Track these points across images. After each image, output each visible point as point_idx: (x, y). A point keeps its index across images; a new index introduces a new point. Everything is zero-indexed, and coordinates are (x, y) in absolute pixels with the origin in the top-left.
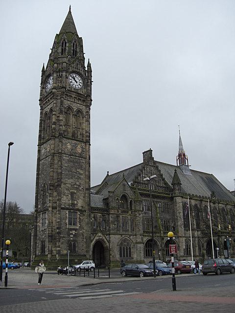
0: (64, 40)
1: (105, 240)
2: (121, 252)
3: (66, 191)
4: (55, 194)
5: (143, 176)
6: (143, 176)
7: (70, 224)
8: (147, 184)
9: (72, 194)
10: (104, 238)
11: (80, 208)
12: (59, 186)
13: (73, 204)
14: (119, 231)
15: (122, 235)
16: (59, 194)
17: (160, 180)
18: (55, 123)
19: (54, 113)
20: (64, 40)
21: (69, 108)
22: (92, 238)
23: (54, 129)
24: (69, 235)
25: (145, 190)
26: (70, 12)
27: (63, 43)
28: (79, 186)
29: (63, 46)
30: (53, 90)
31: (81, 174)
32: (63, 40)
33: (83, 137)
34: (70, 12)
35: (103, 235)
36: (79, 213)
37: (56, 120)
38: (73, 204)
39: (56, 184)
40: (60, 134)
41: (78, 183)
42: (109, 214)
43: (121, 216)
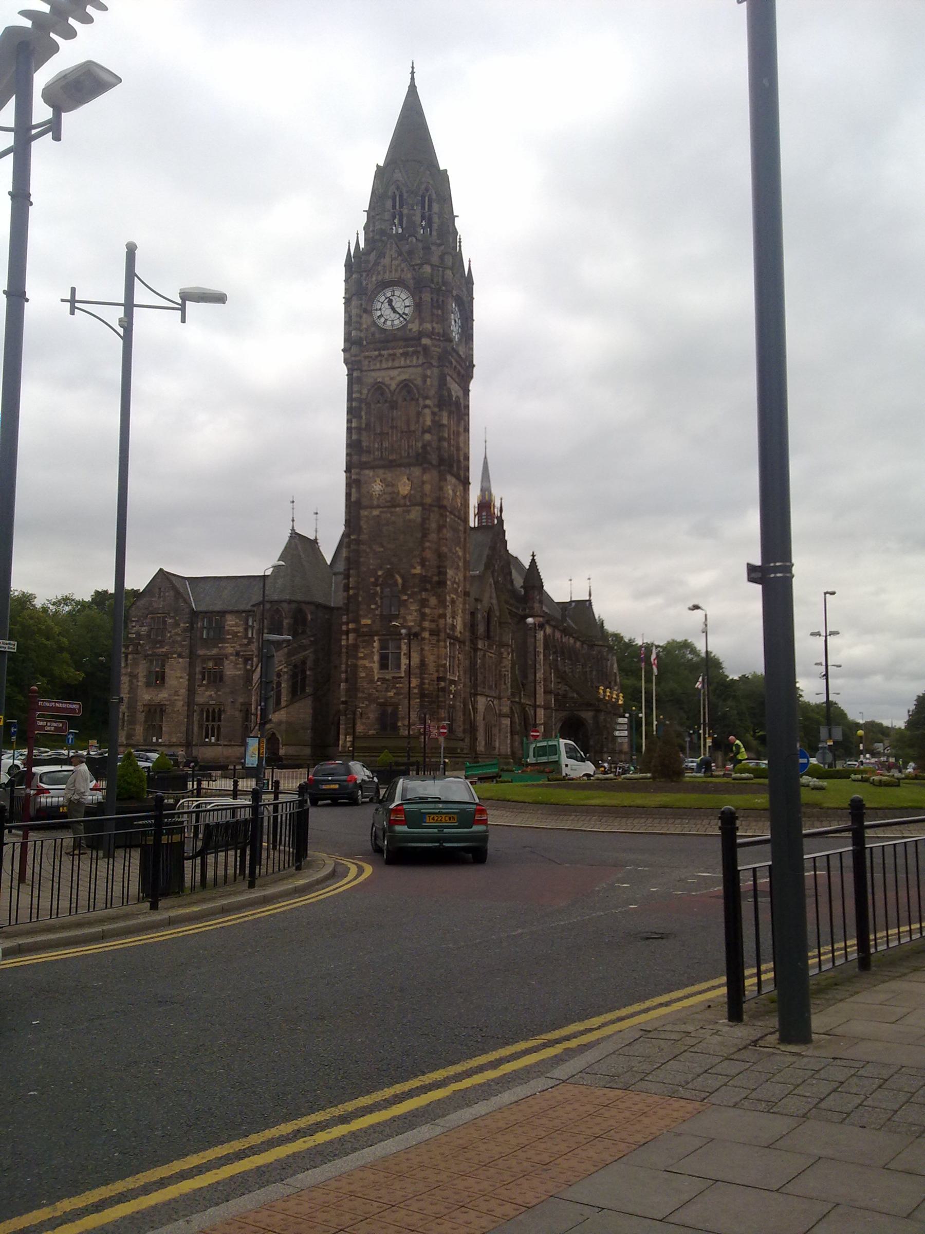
0: (427, 190)
4: (433, 601)
12: (442, 583)
16: (442, 603)
18: (428, 431)
19: (428, 402)
20: (427, 190)
23: (429, 443)
27: (423, 197)
29: (423, 207)
30: (425, 341)
32: (423, 187)
33: (459, 468)
37: (433, 421)
39: (436, 579)
40: (441, 461)
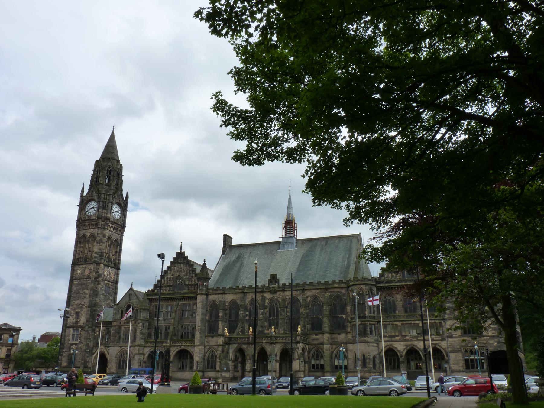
1: (106, 352)
2: (120, 364)
3: (72, 312)
5: (167, 278)
6: (167, 278)
7: (73, 339)
8: (171, 286)
9: (77, 314)
10: (105, 350)
11: (82, 325)
13: (77, 322)
14: (119, 342)
15: (121, 347)
17: (192, 277)
21: (84, 236)
22: (94, 351)
24: (70, 349)
25: (168, 294)
26: (113, 133)
28: (84, 305)
31: (86, 294)
34: (113, 133)
35: (105, 347)
36: (80, 329)
38: (77, 322)
41: (83, 303)
42: (111, 327)
43: (123, 328)
